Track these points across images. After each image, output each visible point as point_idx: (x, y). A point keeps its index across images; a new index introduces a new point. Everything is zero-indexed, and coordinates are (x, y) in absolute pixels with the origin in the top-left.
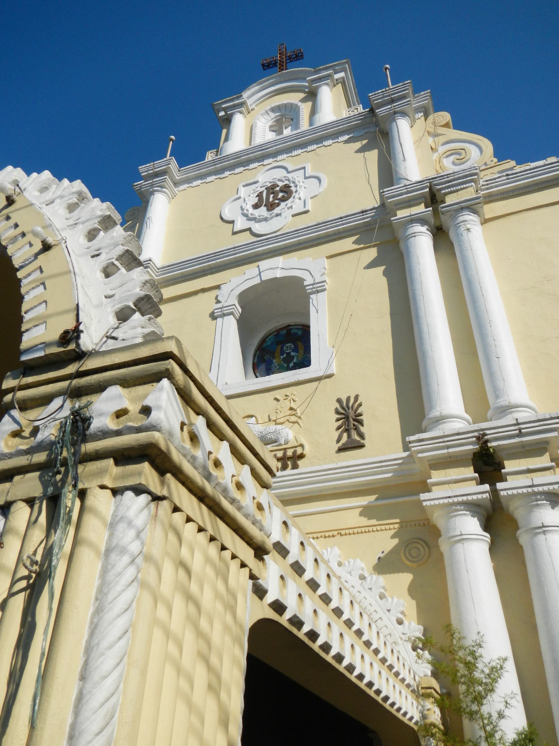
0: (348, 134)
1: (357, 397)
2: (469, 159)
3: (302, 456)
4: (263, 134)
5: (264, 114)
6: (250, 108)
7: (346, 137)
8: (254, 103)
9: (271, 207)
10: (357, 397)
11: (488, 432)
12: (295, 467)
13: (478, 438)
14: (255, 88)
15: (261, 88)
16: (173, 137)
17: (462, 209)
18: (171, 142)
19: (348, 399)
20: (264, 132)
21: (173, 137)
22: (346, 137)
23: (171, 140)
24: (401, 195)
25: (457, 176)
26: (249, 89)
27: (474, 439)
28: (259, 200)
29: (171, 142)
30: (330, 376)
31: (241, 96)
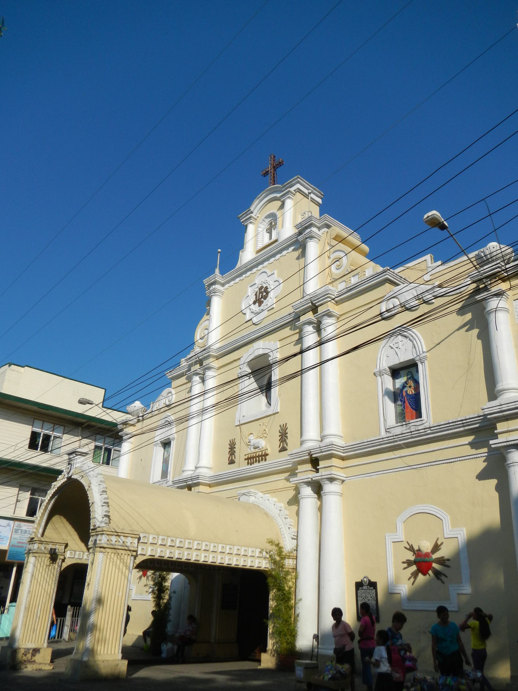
0: (293, 246)
1: (286, 424)
2: (342, 265)
3: (267, 455)
4: (262, 240)
5: (262, 222)
6: (256, 217)
7: (293, 248)
8: (258, 212)
9: (260, 303)
10: (286, 424)
11: (312, 451)
12: (265, 460)
13: (309, 454)
14: (256, 202)
15: (259, 201)
16: (219, 250)
17: (324, 316)
18: (219, 254)
19: (283, 425)
20: (263, 236)
21: (219, 250)
22: (293, 248)
23: (219, 252)
24: (300, 307)
25: (321, 296)
26: (253, 204)
27: (308, 454)
28: (256, 298)
29: (219, 254)
30: (277, 413)
31: (250, 210)
